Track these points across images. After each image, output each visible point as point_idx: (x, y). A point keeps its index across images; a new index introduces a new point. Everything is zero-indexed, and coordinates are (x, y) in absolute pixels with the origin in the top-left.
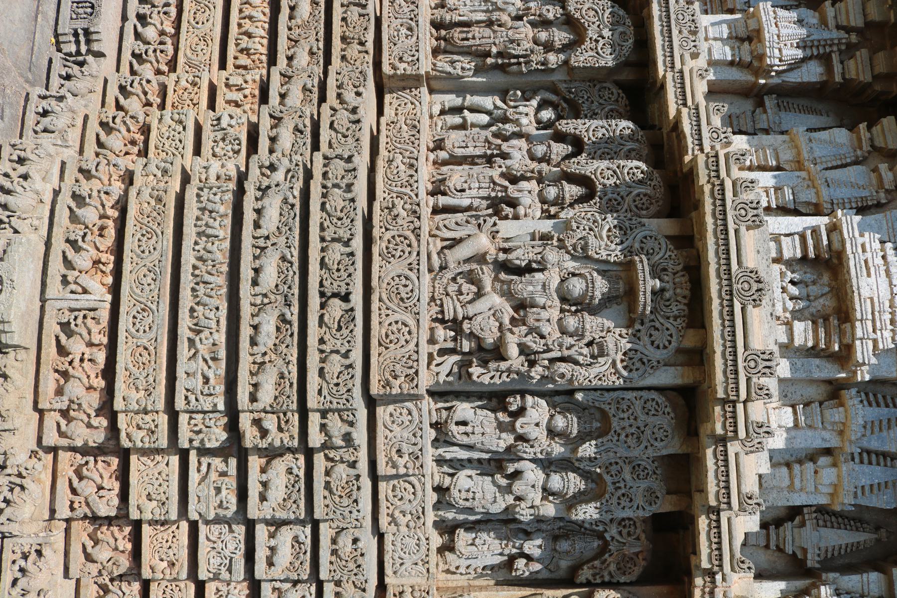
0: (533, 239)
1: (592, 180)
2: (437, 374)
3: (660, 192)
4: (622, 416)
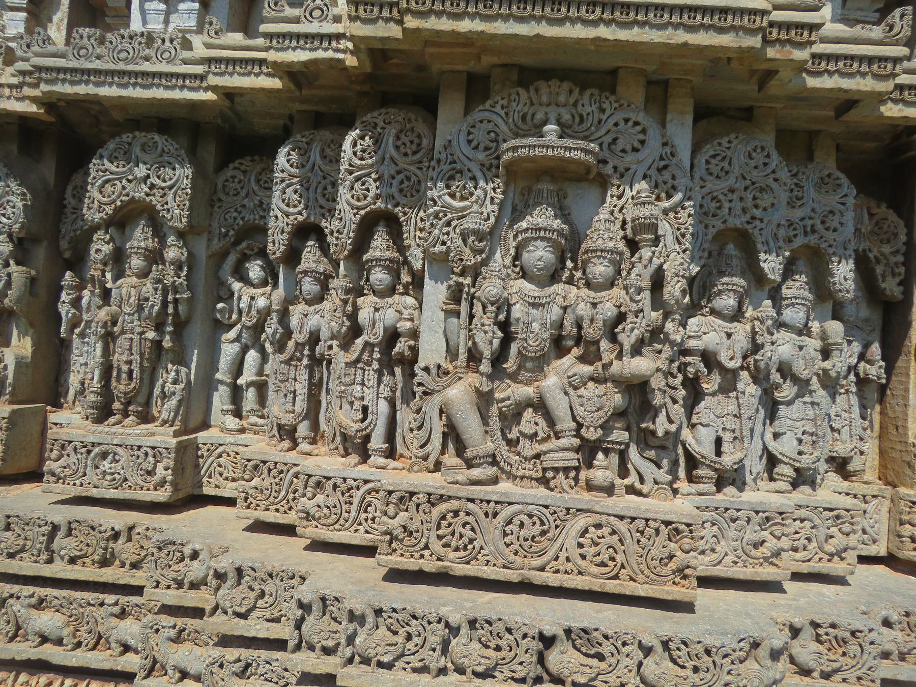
0: (458, 314)
1: (367, 214)
2: (656, 483)
3: (396, 114)
4: (727, 211)
